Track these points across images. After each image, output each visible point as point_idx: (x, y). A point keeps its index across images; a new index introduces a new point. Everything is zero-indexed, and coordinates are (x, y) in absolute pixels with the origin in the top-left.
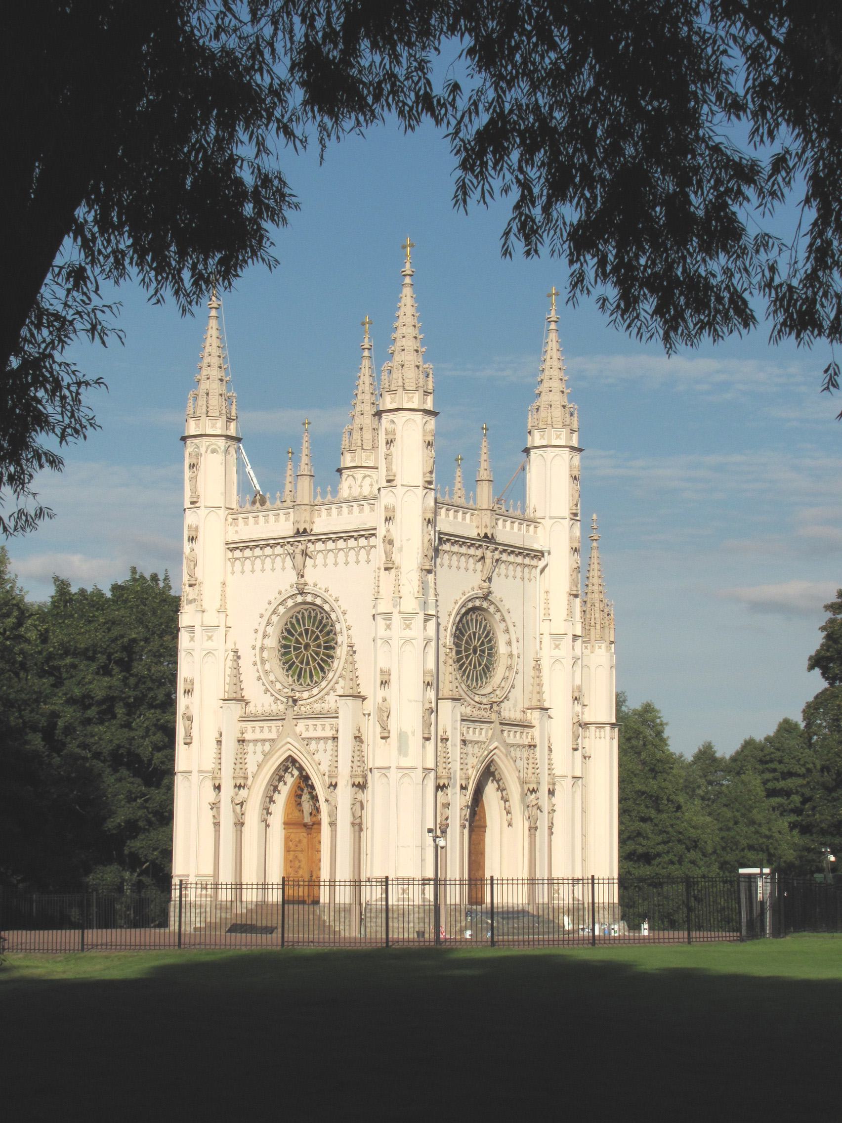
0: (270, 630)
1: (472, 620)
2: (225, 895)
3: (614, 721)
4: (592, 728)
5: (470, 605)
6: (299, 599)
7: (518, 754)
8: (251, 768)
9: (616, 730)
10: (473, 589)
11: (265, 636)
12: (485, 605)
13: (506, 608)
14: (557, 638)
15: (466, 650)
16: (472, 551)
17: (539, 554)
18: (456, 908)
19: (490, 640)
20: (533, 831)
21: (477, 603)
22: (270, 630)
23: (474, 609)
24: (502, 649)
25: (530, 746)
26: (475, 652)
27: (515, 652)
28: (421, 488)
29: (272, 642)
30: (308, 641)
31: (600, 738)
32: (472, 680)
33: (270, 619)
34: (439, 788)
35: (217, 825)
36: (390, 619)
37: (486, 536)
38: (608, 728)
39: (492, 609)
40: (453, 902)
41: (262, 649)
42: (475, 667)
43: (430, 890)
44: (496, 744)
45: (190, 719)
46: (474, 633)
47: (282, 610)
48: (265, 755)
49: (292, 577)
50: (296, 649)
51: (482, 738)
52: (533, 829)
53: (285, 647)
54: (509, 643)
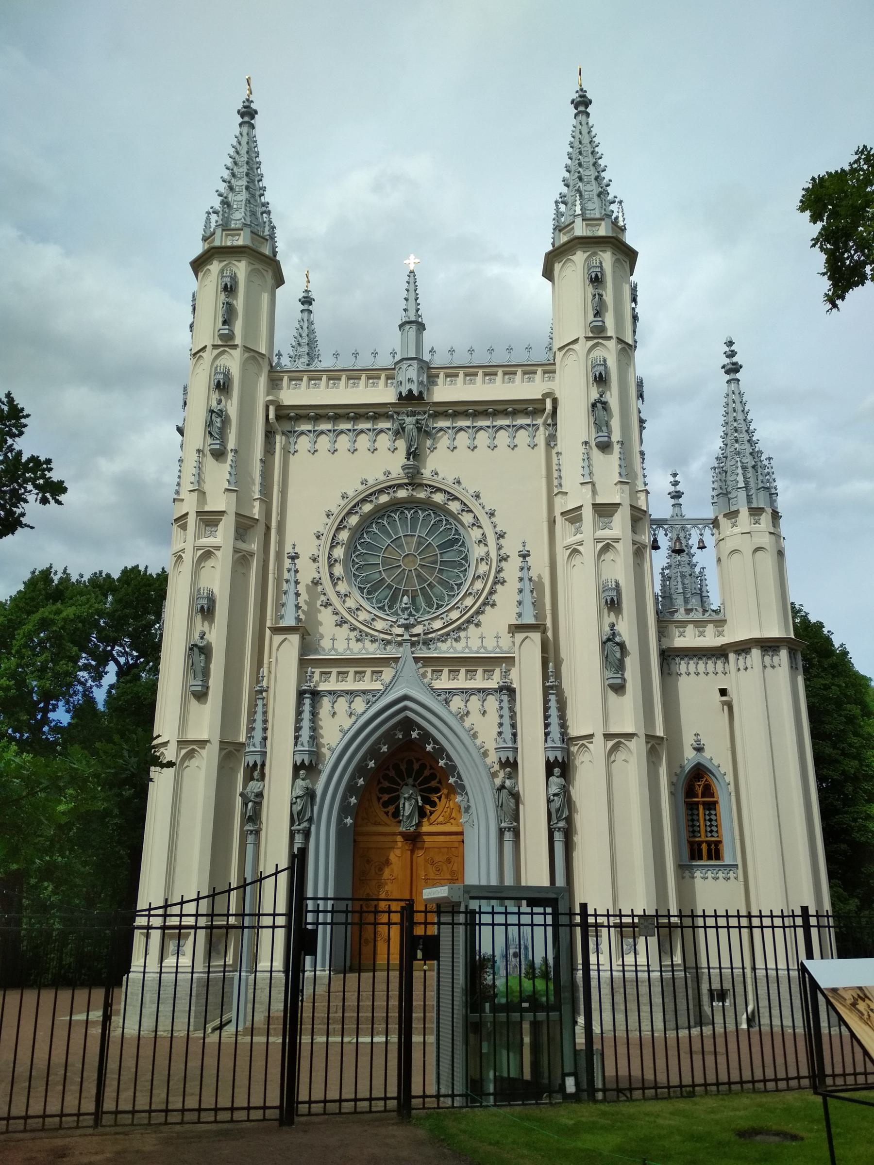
4: (732, 656)
5: (384, 499)
7: (475, 702)
9: (784, 654)
10: (387, 473)
13: (471, 492)
14: (573, 516)
20: (508, 836)
21: (402, 494)
24: (478, 552)
25: (501, 689)
27: (494, 555)
31: (746, 669)
37: (400, 397)
38: (756, 653)
39: (438, 498)
51: (377, 686)
54: (483, 541)
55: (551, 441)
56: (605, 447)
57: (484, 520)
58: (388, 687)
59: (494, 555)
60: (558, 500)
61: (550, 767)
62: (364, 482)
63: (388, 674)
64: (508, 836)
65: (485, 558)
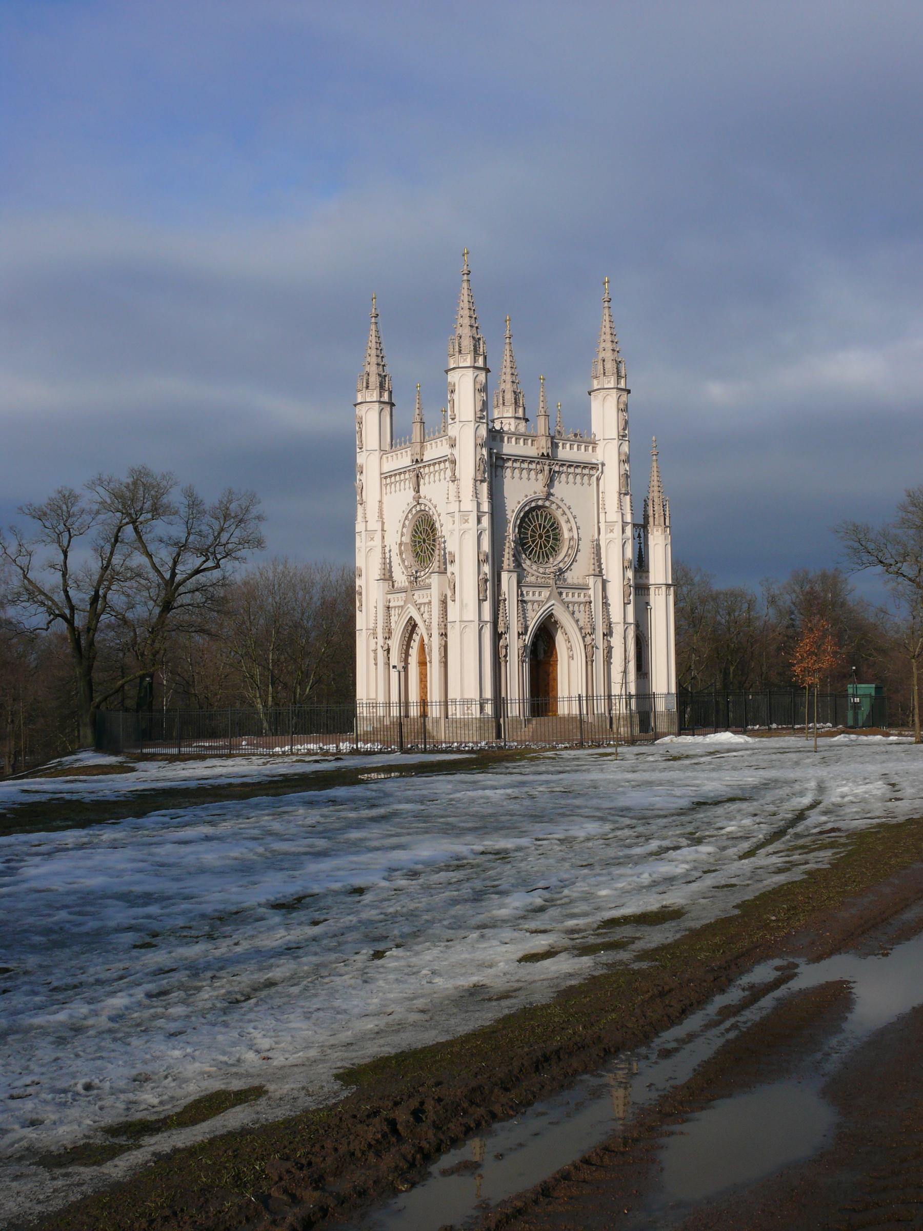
0: (405, 530)
1: (537, 515)
2: (381, 712)
3: (670, 582)
6: (418, 509)
8: (393, 625)
9: (672, 589)
10: (535, 493)
11: (402, 536)
12: (547, 504)
15: (532, 536)
16: (533, 466)
17: (594, 467)
18: (516, 720)
19: (555, 529)
21: (540, 503)
22: (405, 530)
23: (538, 507)
24: (566, 535)
26: (541, 537)
27: (576, 537)
28: (473, 423)
29: (407, 539)
30: (424, 537)
32: (539, 557)
33: (404, 523)
34: (497, 636)
35: (376, 664)
36: (453, 517)
40: (514, 714)
41: (400, 544)
42: (541, 548)
43: (489, 709)
44: (553, 602)
45: (361, 594)
46: (540, 525)
47: (410, 516)
48: (399, 615)
49: (413, 493)
50: (419, 542)
51: (542, 598)
52: (590, 661)
53: (415, 541)
55: (598, 485)
56: (625, 494)
57: (572, 519)
58: (548, 599)
59: (576, 537)
60: (602, 516)
61: (604, 635)
62: (526, 496)
63: (545, 593)
64: (589, 663)
65: (571, 539)
